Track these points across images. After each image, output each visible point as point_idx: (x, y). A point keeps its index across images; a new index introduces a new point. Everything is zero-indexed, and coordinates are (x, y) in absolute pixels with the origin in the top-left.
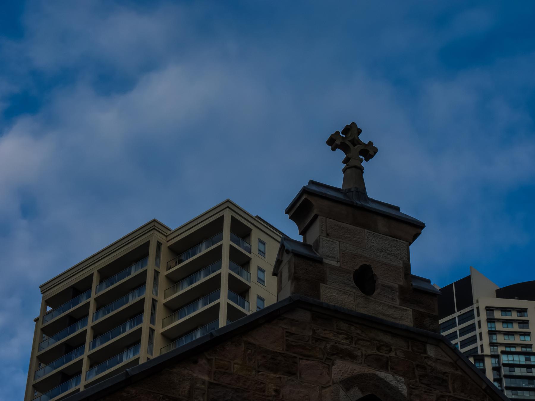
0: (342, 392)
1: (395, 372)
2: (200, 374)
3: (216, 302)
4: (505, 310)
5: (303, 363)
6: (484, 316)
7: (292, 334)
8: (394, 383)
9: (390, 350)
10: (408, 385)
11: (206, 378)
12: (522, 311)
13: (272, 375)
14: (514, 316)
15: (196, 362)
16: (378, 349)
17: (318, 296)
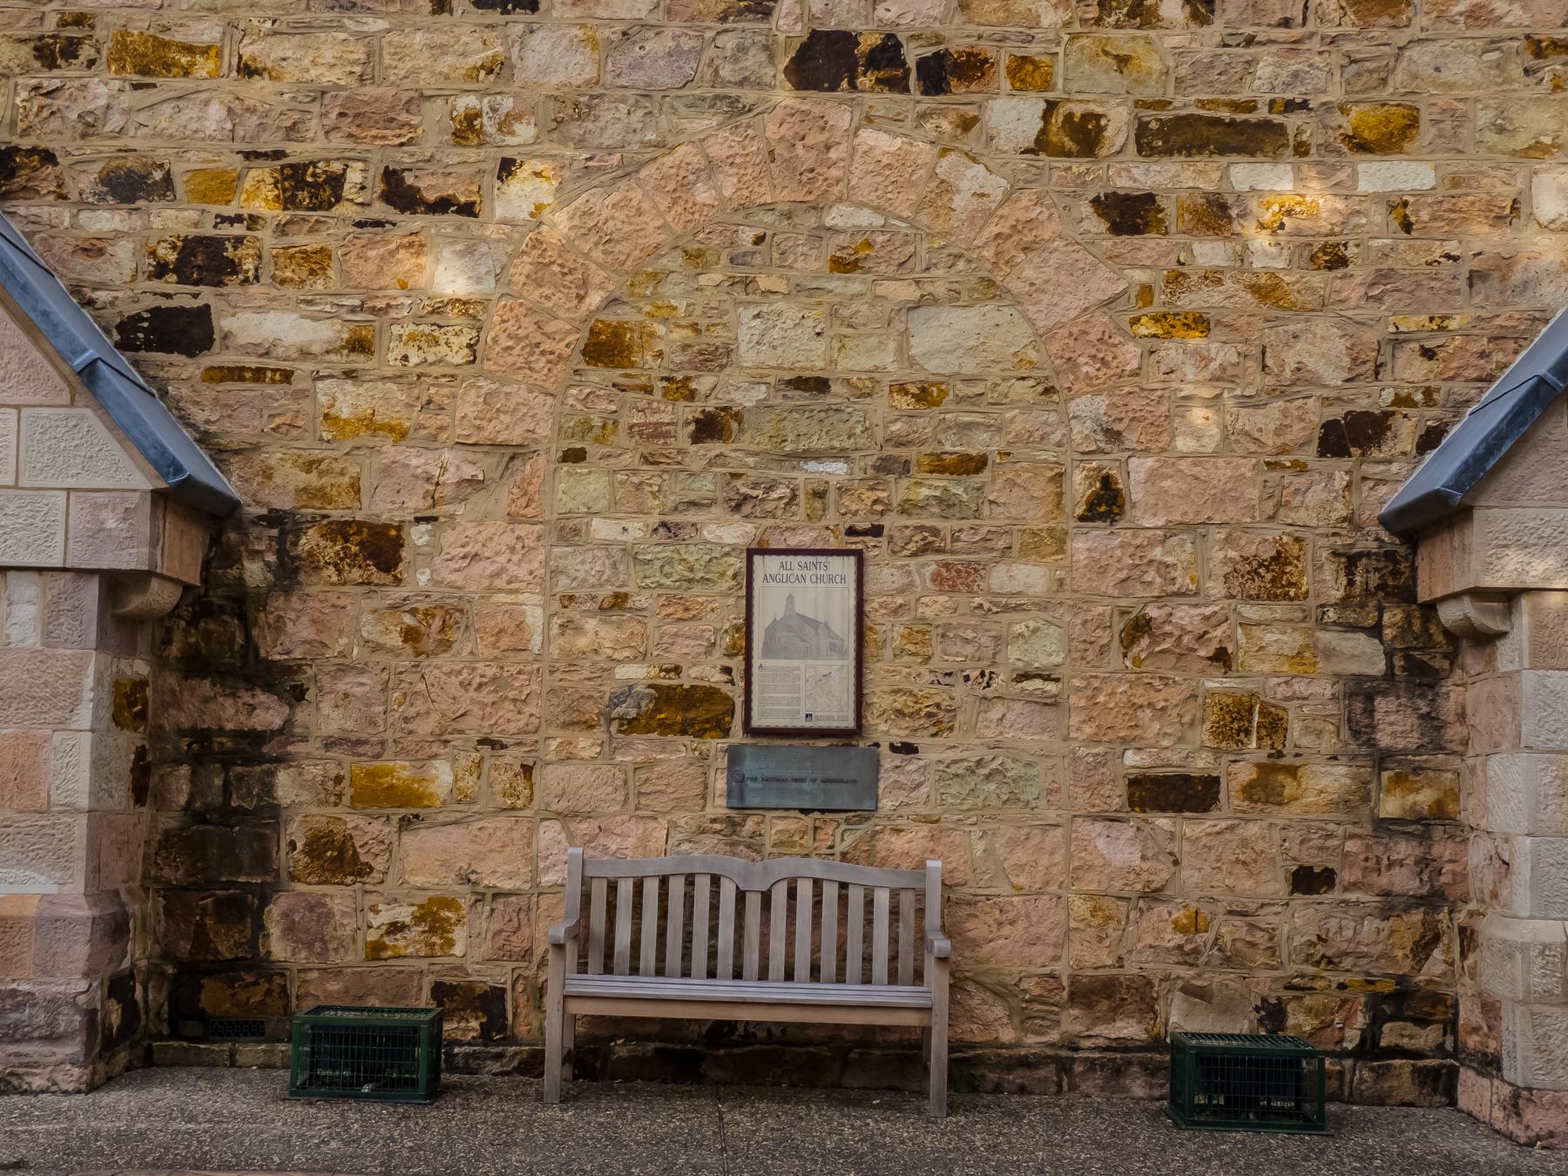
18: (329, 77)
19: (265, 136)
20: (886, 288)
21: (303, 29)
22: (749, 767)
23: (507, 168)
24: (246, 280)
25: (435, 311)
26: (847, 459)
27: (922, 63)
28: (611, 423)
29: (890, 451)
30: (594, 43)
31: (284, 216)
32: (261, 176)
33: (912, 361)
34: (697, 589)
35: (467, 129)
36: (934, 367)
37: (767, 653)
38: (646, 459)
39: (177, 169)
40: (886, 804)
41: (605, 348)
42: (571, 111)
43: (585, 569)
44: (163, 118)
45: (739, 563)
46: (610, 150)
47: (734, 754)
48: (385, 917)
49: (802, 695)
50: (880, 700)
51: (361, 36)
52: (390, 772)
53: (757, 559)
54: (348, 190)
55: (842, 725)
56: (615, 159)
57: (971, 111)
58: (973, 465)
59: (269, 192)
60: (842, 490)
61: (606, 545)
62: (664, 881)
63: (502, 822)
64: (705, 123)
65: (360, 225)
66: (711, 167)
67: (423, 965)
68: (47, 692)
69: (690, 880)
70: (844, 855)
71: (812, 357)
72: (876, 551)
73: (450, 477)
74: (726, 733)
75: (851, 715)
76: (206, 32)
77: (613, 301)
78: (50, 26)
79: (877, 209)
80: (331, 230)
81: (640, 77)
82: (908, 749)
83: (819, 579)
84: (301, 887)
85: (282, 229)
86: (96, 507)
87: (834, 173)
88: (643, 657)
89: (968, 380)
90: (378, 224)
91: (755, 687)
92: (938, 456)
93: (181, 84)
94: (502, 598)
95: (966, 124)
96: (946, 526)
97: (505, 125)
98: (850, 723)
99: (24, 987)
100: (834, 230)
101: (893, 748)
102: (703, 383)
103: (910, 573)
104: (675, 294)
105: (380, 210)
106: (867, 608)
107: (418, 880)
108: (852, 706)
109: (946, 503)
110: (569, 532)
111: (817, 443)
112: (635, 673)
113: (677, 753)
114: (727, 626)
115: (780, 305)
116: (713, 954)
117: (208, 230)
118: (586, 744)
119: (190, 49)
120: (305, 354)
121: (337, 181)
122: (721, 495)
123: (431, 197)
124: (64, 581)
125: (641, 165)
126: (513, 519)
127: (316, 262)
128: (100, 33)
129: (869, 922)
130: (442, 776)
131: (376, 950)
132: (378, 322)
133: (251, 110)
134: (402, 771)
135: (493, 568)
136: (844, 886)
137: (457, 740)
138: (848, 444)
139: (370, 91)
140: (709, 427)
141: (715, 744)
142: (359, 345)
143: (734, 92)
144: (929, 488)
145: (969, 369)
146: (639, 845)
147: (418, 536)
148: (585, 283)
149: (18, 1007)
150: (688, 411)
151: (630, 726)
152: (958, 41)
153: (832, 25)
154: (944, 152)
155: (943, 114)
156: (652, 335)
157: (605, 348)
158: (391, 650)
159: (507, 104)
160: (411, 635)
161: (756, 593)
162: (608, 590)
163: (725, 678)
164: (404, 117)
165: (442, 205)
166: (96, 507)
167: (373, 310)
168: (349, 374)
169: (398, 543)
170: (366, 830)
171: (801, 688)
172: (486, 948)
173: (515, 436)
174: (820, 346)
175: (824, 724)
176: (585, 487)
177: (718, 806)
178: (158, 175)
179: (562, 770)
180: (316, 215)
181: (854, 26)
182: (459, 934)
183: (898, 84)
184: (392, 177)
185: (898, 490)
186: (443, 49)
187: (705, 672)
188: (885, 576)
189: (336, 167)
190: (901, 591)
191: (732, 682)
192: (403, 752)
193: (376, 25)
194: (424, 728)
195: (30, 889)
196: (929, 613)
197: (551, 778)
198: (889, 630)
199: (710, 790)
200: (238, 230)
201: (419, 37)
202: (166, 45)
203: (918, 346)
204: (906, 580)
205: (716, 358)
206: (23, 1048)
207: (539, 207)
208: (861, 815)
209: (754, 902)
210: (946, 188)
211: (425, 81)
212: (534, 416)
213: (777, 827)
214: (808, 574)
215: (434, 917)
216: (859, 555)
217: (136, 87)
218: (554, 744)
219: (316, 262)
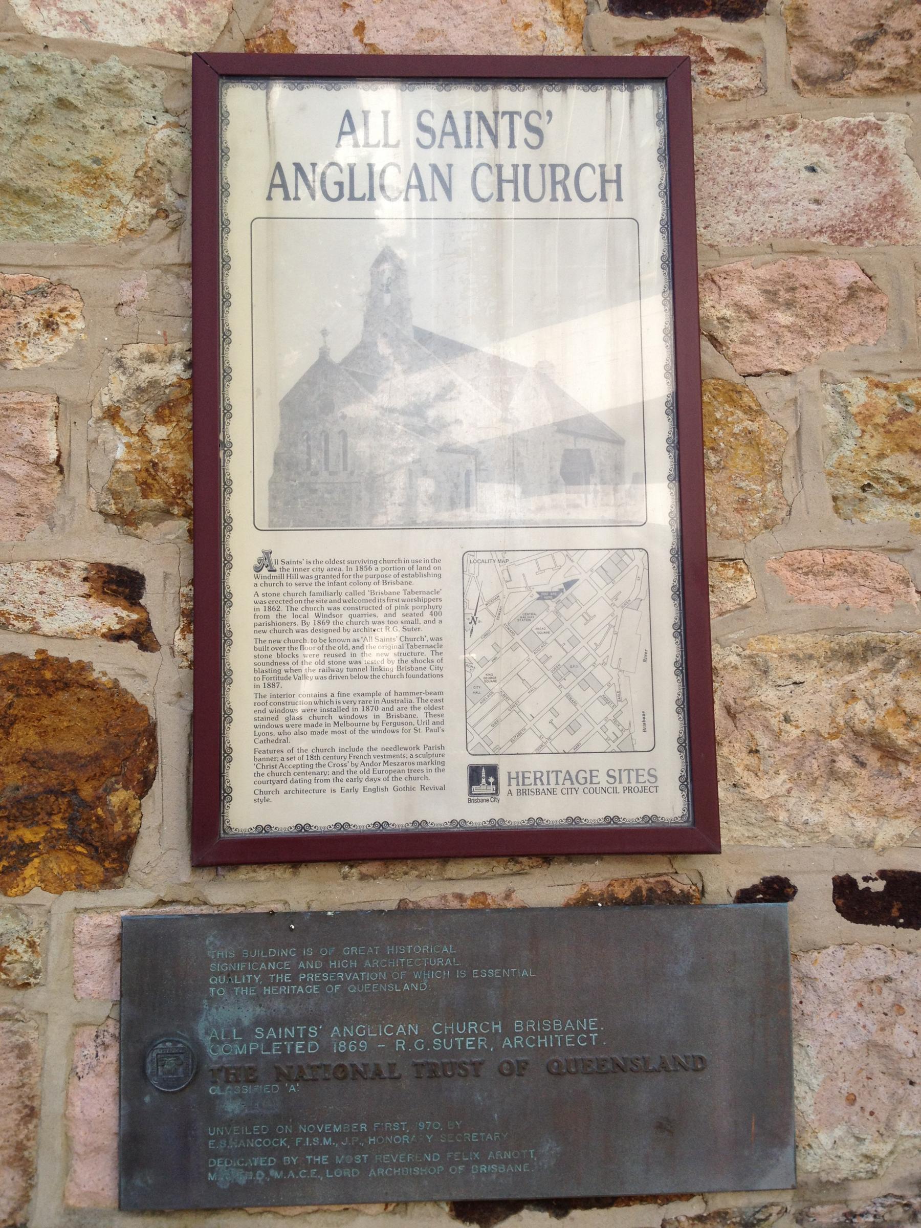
49: (451, 684)
50: (787, 695)
53: (239, 100)
55: (631, 809)
72: (742, 75)
75: (670, 764)
83: (506, 183)
91: (241, 657)
98: (669, 804)
101: (852, 900)
103: (882, 162)
106: (713, 306)
108: (671, 725)
114: (116, 388)
161: (236, 244)
163: (111, 615)
175: (552, 810)
190: (849, 234)
191: (141, 635)
199: (49, 1133)
204: (869, 192)
214: (465, 161)
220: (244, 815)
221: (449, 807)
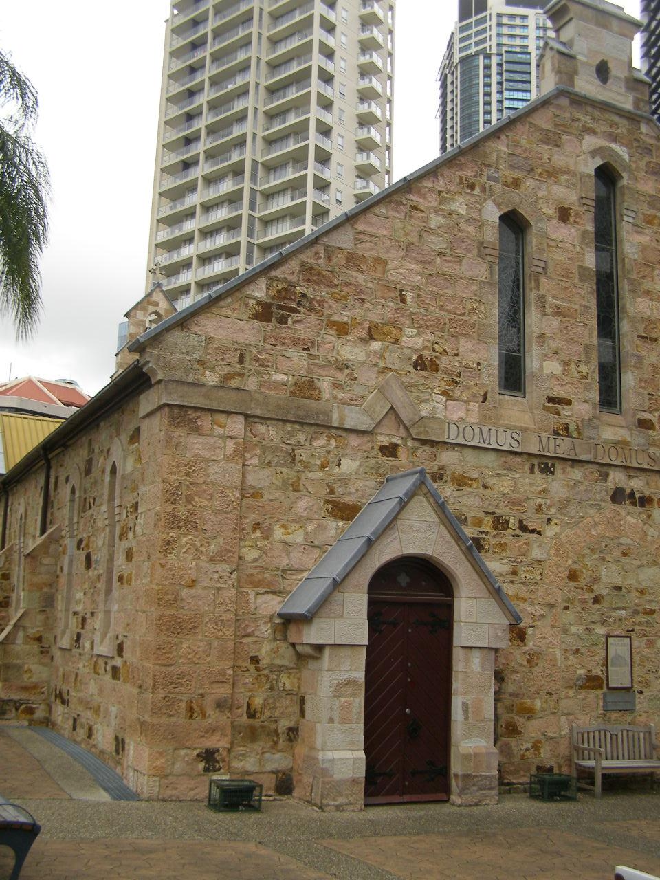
0: (590, 160)
1: (622, 144)
2: (501, 147)
3: (311, 12)
4: (512, 16)
5: (565, 137)
6: (494, 21)
7: (557, 116)
8: (621, 153)
9: (618, 128)
10: (629, 154)
11: (506, 150)
12: (524, 17)
13: (546, 147)
14: (518, 22)
15: (499, 138)
16: (611, 127)
17: (573, 85)
18: (507, 490)
19: (490, 507)
20: (633, 562)
21: (499, 475)
22: (609, 699)
23: (549, 521)
24: (486, 552)
25: (533, 564)
26: (626, 610)
27: (639, 498)
28: (574, 597)
29: (636, 608)
30: (568, 485)
31: (495, 532)
32: (488, 520)
33: (639, 583)
34: (595, 647)
35: (539, 509)
36: (645, 584)
37: (612, 666)
38: (583, 609)
39: (469, 516)
40: (637, 708)
41: (573, 576)
42: (563, 505)
43: (570, 640)
44: (465, 500)
45: (604, 640)
46: (573, 517)
47: (605, 695)
48: (523, 748)
50: (636, 679)
51: (514, 478)
52: (524, 703)
54: (511, 526)
56: (573, 521)
57: (650, 513)
58: (652, 612)
59: (490, 524)
60: (626, 619)
61: (574, 634)
62: (588, 733)
63: (552, 717)
64: (593, 511)
65: (513, 536)
66: (596, 524)
67: (534, 760)
68: (483, 685)
69: (588, 733)
70: (629, 724)
71: (618, 581)
73: (537, 614)
74: (602, 689)
76: (475, 475)
77: (575, 562)
78: (435, 469)
79: (632, 539)
80: (507, 537)
81: (578, 497)
82: (641, 692)
84: (503, 739)
85: (495, 536)
86: (495, 628)
87: (622, 528)
88: (583, 667)
89: (652, 588)
90: (518, 536)
92: (645, 610)
93: (469, 489)
94: (551, 650)
95: (649, 516)
96: (648, 629)
97: (548, 509)
99: (483, 774)
100: (622, 544)
102: (595, 587)
104: (587, 561)
105: (518, 532)
107: (533, 735)
109: (647, 622)
110: (565, 631)
111: (620, 605)
112: (581, 672)
113: (592, 696)
115: (611, 565)
116: (623, 755)
117: (475, 535)
118: (571, 693)
119: (471, 479)
120: (501, 575)
121: (508, 522)
122: (599, 620)
123: (530, 528)
124: (486, 651)
125: (579, 522)
126: (553, 626)
127: (503, 547)
128: (448, 472)
129: (639, 741)
130: (538, 704)
131: (523, 756)
132: (519, 565)
133: (487, 499)
134: (528, 702)
135: (548, 641)
136: (628, 731)
137: (541, 693)
138: (627, 605)
139: (515, 496)
140: (597, 600)
141: (601, 692)
142: (515, 573)
143: (600, 503)
144: (644, 618)
145: (652, 585)
146: (586, 722)
147: (530, 631)
148: (567, 557)
149: (481, 780)
150: (592, 595)
151: (581, 687)
152: (647, 494)
153: (620, 486)
154: (645, 524)
155: (644, 513)
156: (582, 573)
157: (573, 576)
158: (524, 666)
159: (549, 502)
160: (529, 661)
162: (575, 648)
164: (523, 504)
165: (533, 531)
166: (495, 628)
167: (518, 562)
168: (512, 582)
169: (525, 634)
170: (520, 721)
171: (619, 677)
172: (549, 755)
173: (552, 602)
174: (620, 578)
176: (570, 617)
177: (601, 711)
178: (463, 518)
179: (565, 701)
180: (503, 532)
181: (625, 487)
182: (542, 751)
183: (634, 504)
184: (521, 522)
185: (638, 619)
186: (532, 484)
187: (597, 671)
188: (635, 644)
189: (507, 518)
190: (639, 648)
192: (529, 697)
193: (517, 476)
194: (533, 689)
195: (481, 744)
196: (645, 654)
197: (563, 703)
198: (637, 659)
200: (484, 536)
201: (527, 480)
202: (465, 477)
203: (642, 577)
205: (597, 580)
206: (484, 792)
207: (556, 533)
208: (632, 711)
209: (614, 737)
210: (646, 534)
211: (528, 494)
212: (558, 597)
213: (614, 715)
215: (536, 746)
216: (630, 637)
217: (458, 490)
218: (564, 693)
219: (503, 547)
220: (610, 686)
221: (620, 686)
